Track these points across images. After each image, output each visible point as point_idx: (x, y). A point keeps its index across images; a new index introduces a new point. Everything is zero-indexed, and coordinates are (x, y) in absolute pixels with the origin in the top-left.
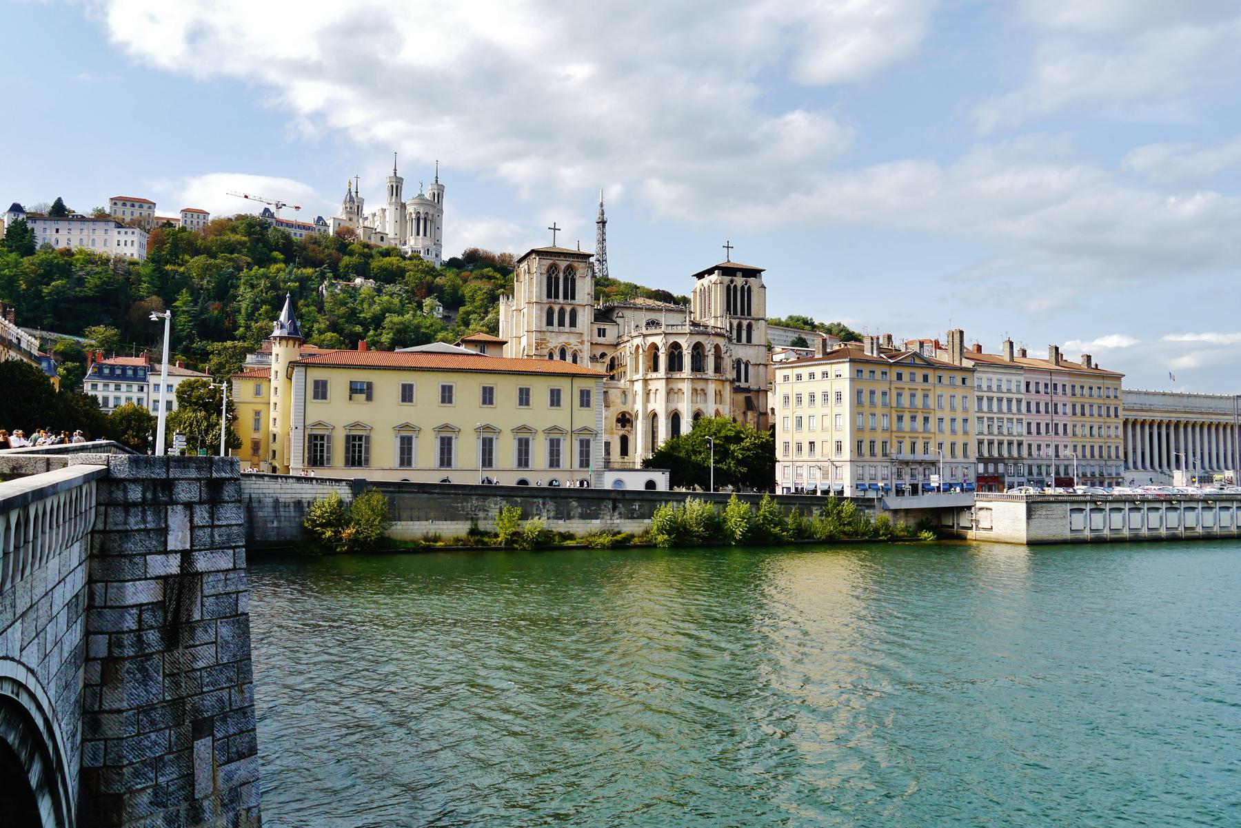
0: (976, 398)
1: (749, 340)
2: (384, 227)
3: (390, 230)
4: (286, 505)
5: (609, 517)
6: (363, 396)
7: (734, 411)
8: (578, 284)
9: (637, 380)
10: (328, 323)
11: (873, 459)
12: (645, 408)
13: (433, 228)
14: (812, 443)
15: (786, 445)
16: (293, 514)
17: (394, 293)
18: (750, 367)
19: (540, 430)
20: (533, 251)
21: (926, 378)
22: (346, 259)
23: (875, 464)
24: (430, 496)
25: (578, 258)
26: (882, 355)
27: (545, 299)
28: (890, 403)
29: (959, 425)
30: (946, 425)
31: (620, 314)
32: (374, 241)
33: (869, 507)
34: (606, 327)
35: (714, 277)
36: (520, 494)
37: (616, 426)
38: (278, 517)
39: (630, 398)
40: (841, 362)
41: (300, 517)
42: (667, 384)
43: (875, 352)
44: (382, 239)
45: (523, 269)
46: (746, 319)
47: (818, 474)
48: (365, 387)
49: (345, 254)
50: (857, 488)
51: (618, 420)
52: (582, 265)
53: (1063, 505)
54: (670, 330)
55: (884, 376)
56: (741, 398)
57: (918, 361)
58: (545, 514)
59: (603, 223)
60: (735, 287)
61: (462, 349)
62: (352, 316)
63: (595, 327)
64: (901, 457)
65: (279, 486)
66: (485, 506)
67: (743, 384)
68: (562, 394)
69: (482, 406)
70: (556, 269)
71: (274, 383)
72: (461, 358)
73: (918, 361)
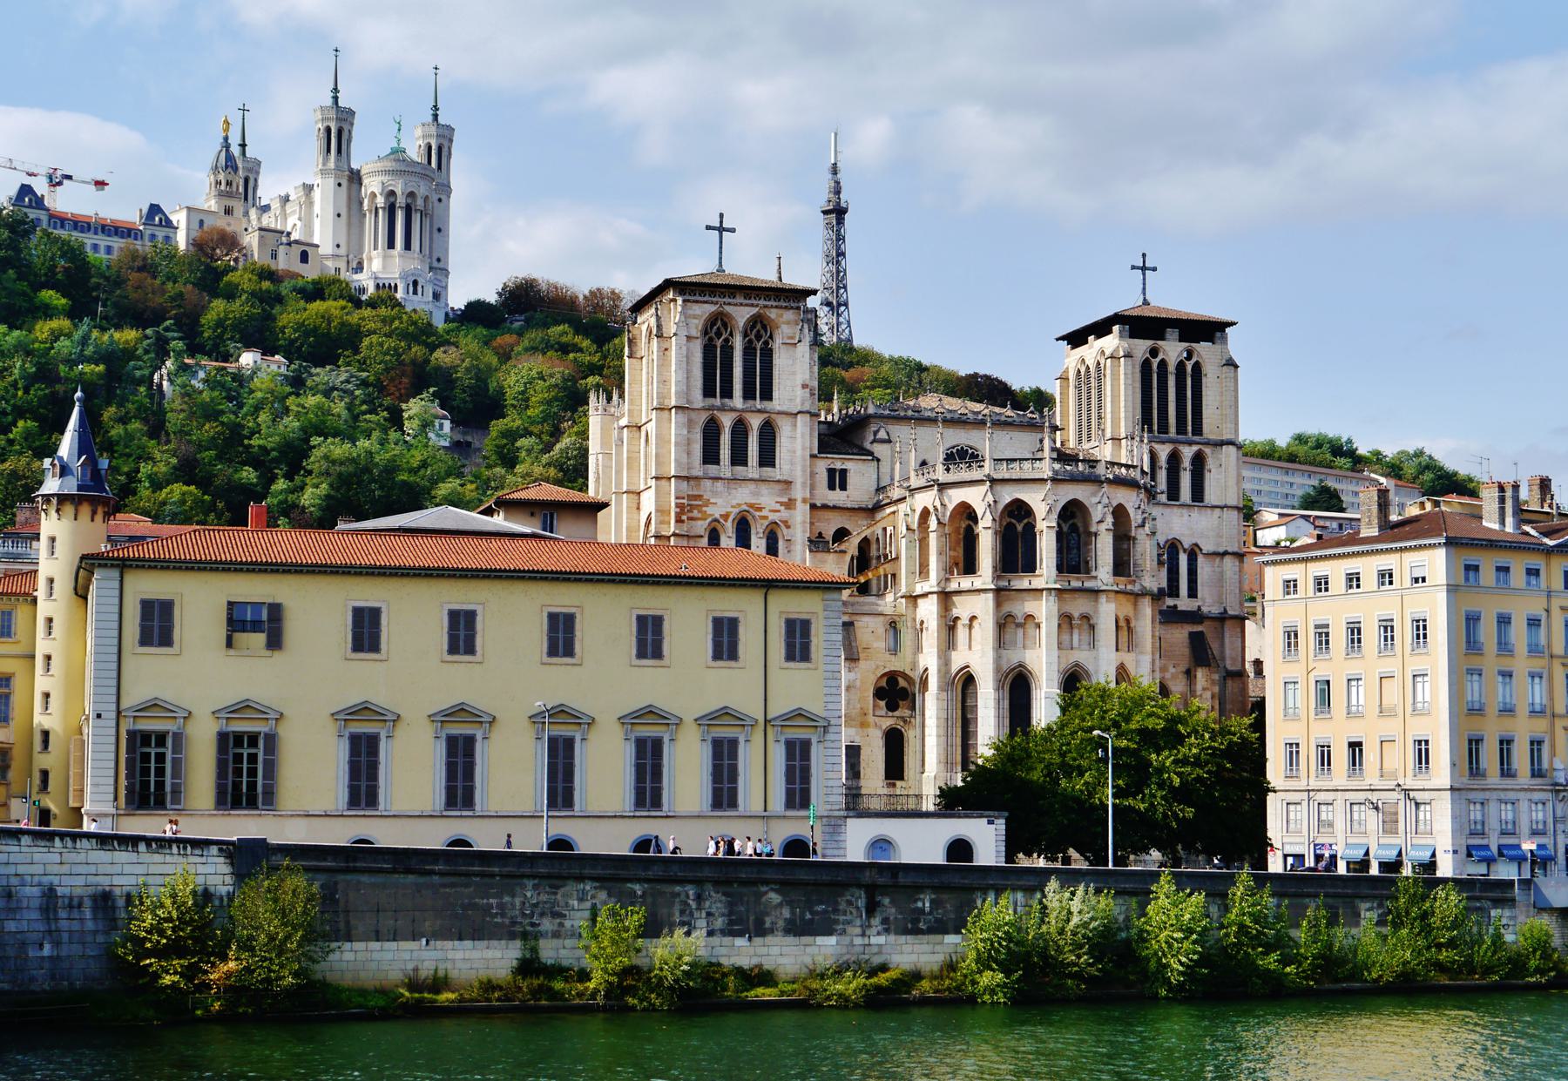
1: (1198, 493)
2: (308, 227)
3: (323, 234)
4: (74, 904)
5: (858, 930)
6: (260, 639)
7: (1163, 669)
8: (781, 360)
9: (925, 595)
10: (174, 461)
11: (1508, 783)
12: (945, 661)
14: (1355, 746)
15: (1293, 750)
16: (90, 925)
17: (334, 389)
18: (1200, 559)
19: (688, 718)
20: (668, 284)
22: (218, 306)
23: (1511, 796)
24: (421, 880)
25: (777, 298)
26: (1527, 528)
27: (698, 399)
28: (1549, 646)
31: (882, 435)
32: (286, 261)
33: (1499, 902)
34: (848, 465)
35: (1111, 342)
36: (643, 874)
37: (874, 706)
38: (53, 935)
39: (907, 637)
40: (1426, 547)
41: (107, 933)
42: (998, 604)
43: (1509, 520)
44: (304, 257)
45: (644, 328)
46: (1190, 443)
47: (1372, 820)
48: (265, 616)
49: (215, 294)
50: (1469, 855)
51: (879, 693)
52: (789, 315)
54: (1003, 472)
55: (1533, 580)
56: (1179, 635)
58: (702, 923)
59: (837, 213)
60: (1163, 364)
61: (499, 521)
62: (233, 442)
63: (822, 466)
65: (56, 858)
66: (555, 903)
67: (1184, 603)
68: (741, 630)
69: (546, 659)
70: (725, 325)
71: (44, 608)
72: (495, 544)
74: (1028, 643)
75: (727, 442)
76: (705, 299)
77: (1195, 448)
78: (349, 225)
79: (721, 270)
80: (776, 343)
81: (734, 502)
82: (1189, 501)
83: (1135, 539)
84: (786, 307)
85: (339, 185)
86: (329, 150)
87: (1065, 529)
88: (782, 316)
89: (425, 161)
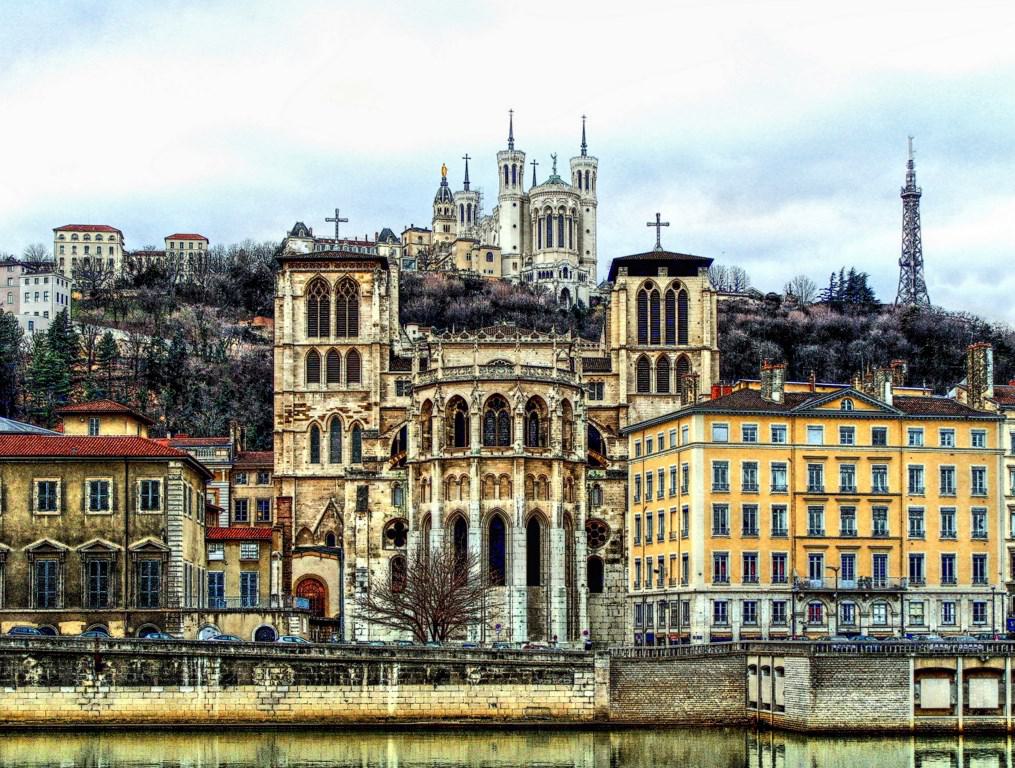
0: (1006, 471)
13: (575, 231)
21: (879, 438)
27: (303, 338)
29: (963, 524)
30: (932, 524)
37: (385, 543)
42: (444, 470)
44: (490, 257)
46: (675, 351)
52: (367, 277)
53: (900, 663)
57: (857, 406)
59: (911, 197)
60: (656, 294)
63: (391, 380)
64: (816, 583)
73: (857, 406)
74: (464, 495)
77: (679, 353)
78: (522, 233)
79: (659, 245)
81: (328, 408)
83: (551, 419)
84: (365, 271)
85: (515, 205)
86: (507, 182)
88: (362, 277)
89: (577, 185)
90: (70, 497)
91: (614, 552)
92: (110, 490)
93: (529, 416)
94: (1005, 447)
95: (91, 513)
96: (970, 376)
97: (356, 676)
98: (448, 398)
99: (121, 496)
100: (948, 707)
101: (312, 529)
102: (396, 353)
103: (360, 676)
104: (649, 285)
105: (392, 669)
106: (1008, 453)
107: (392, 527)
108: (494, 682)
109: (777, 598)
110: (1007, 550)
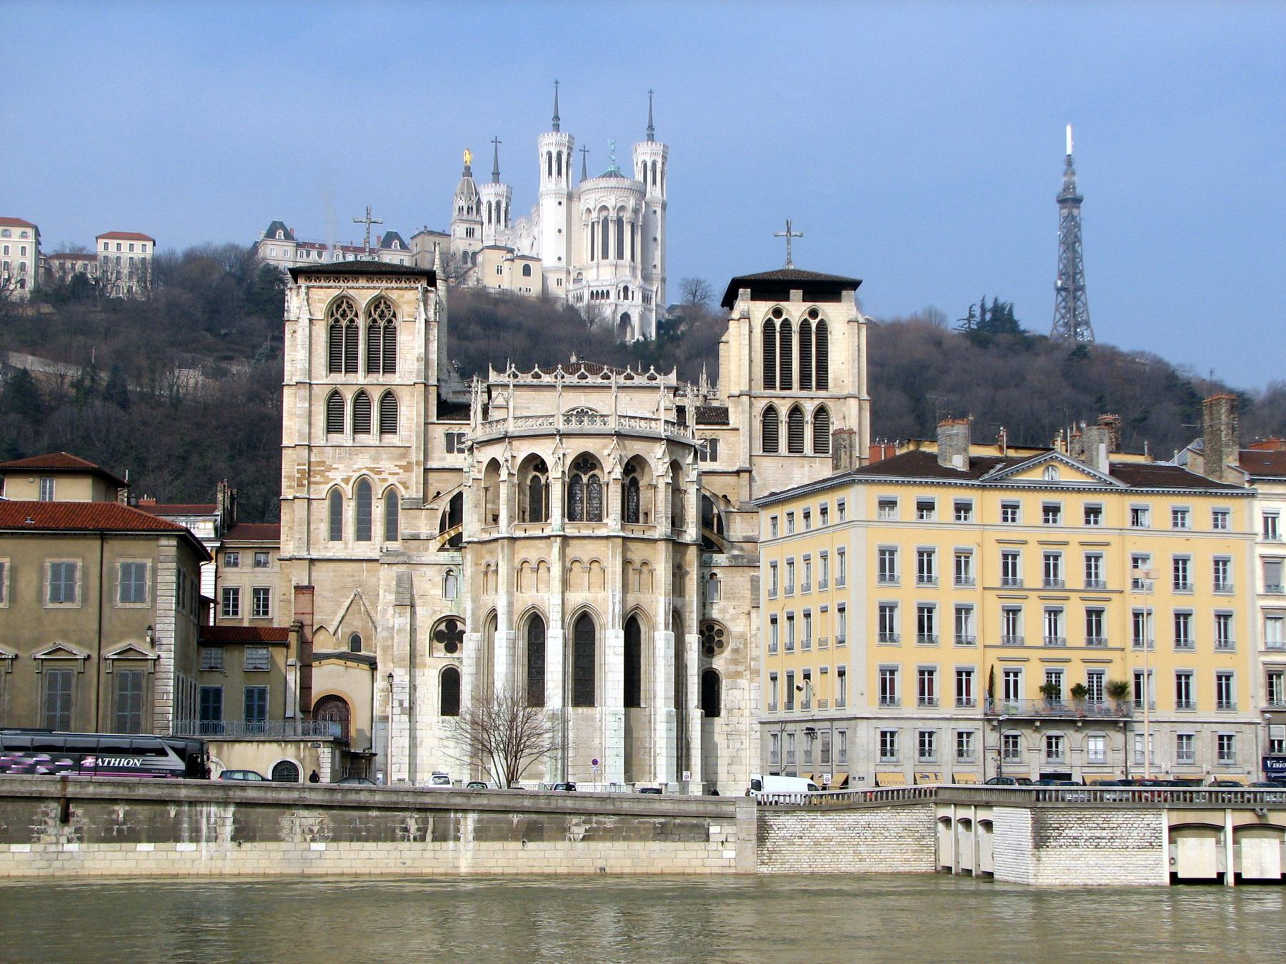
0: (1258, 563)
5: (54, 839)
27: (321, 376)
29: (1203, 629)
34: (465, 430)
44: (527, 272)
51: (437, 636)
52: (411, 295)
53: (1149, 817)
59: (1070, 200)
60: (786, 324)
63: (439, 432)
70: (350, 307)
75: (349, 413)
76: (329, 285)
77: (817, 402)
80: (398, 323)
81: (355, 467)
82: (811, 453)
84: (406, 288)
85: (560, 203)
86: (550, 173)
87: (585, 479)
88: (403, 296)
90: (22, 584)
91: (736, 662)
92: (78, 574)
93: (627, 481)
94: (1256, 531)
95: (51, 606)
96: (1206, 437)
97: (418, 829)
98: (521, 457)
99: (94, 583)
100: (1215, 876)
101: (331, 630)
102: (443, 397)
103: (423, 830)
104: (778, 313)
105: (466, 818)
106: (1260, 538)
107: (443, 627)
108: (602, 839)
109: (963, 726)
110: (1261, 667)
